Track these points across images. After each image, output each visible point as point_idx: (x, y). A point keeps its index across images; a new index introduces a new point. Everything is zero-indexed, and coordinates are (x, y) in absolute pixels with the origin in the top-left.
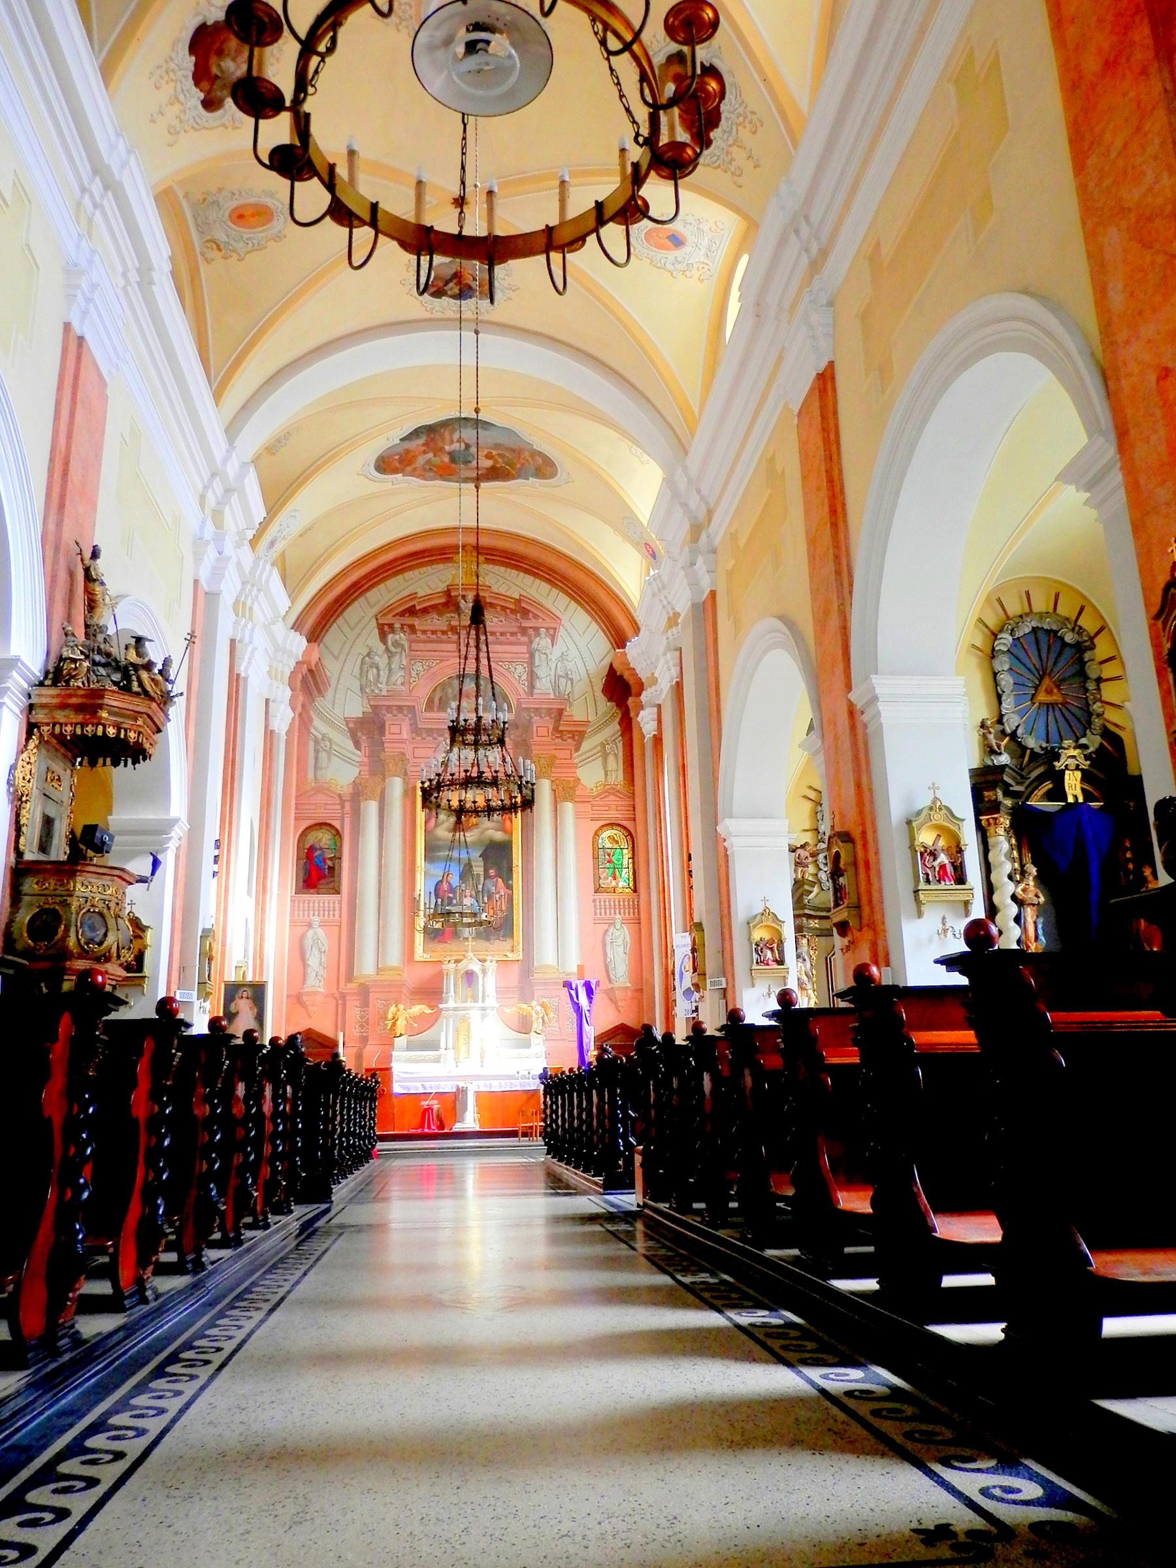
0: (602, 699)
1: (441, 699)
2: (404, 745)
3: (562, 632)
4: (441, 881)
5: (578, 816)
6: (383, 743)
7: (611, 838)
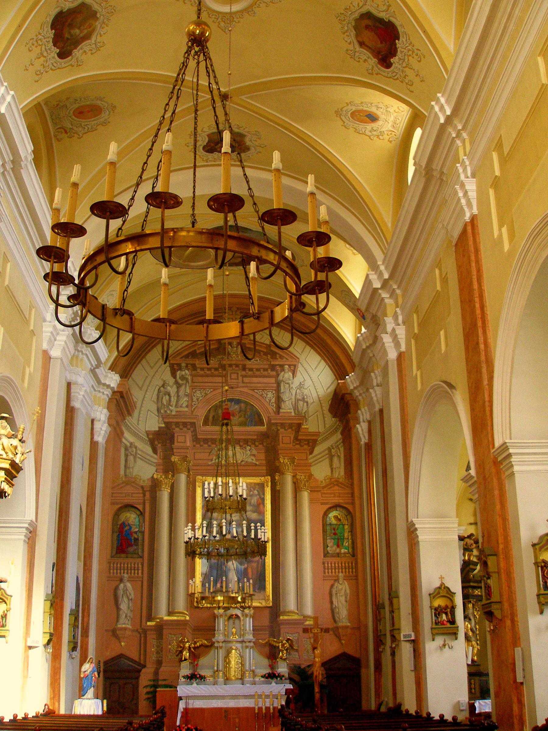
0: (328, 416)
1: (214, 417)
2: (188, 451)
3: (300, 368)
5: (311, 501)
6: (173, 449)
7: (336, 517)
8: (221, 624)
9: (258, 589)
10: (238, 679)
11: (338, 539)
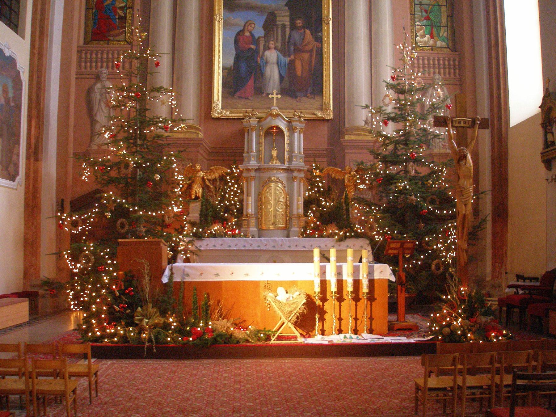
4: (243, 31)
8: (254, 142)
9: (310, 93)
10: (279, 228)
11: (432, 26)
